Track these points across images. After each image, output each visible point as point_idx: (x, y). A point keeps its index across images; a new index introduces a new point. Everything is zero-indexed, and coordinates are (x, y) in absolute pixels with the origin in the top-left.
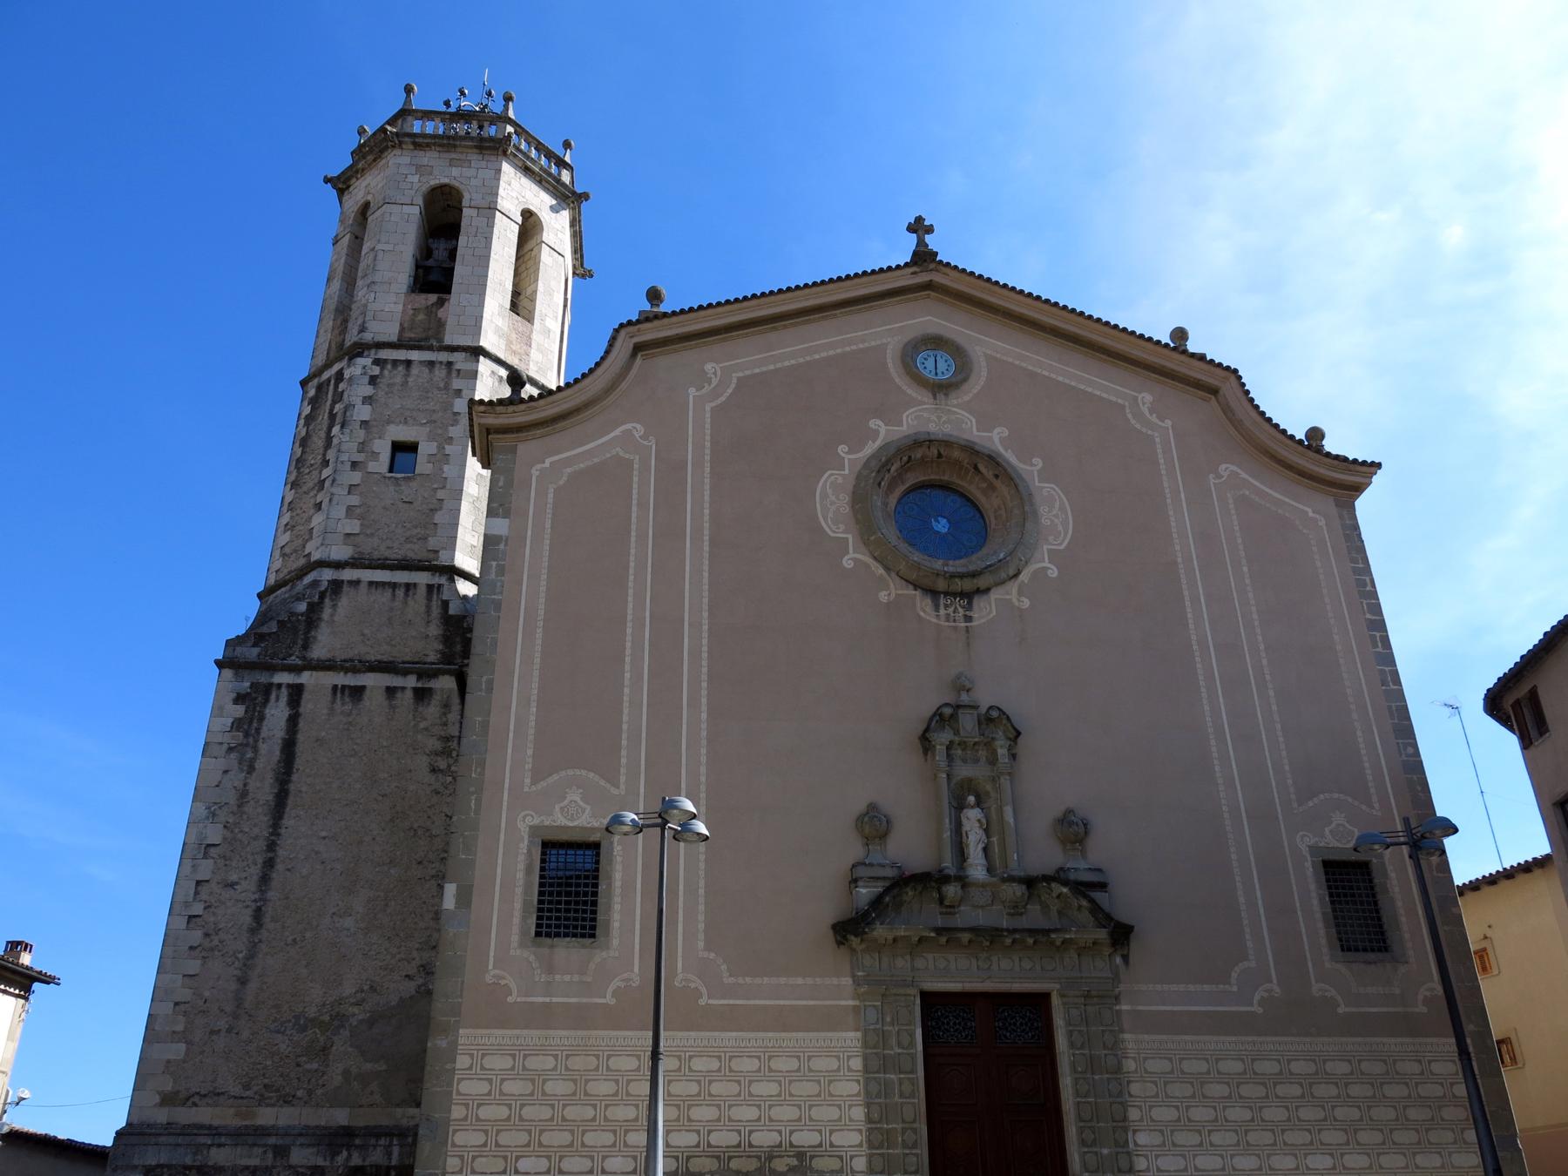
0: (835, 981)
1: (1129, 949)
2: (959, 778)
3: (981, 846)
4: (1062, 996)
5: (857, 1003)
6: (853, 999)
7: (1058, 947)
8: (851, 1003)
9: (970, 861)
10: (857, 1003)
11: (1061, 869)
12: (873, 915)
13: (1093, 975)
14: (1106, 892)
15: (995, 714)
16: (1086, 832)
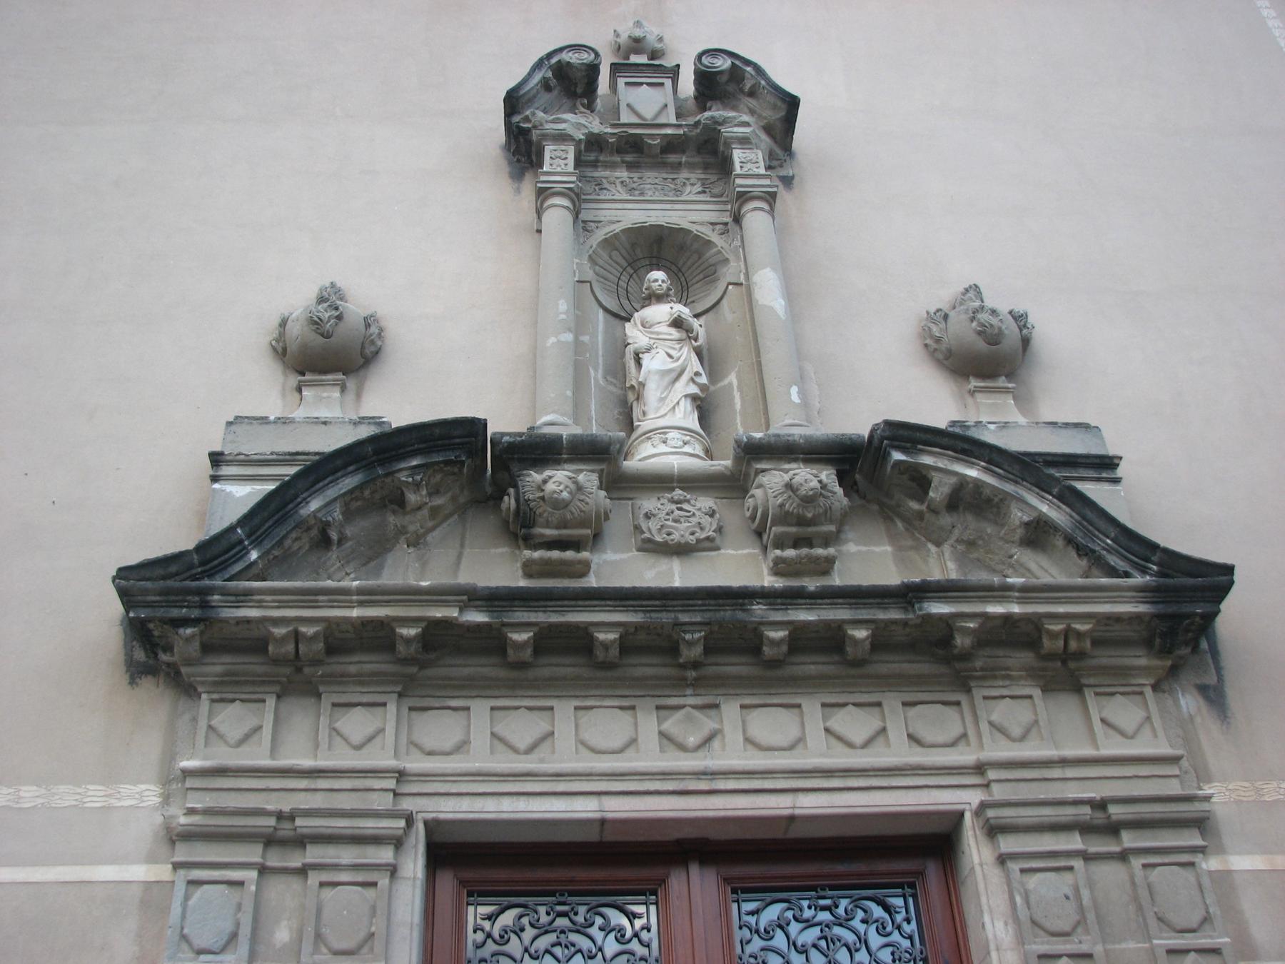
0: (95, 796)
1: (1219, 669)
2: (618, 228)
3: (684, 387)
4: (994, 831)
5: (162, 872)
6: (151, 859)
7: (965, 656)
8: (139, 872)
9: (644, 426)
10: (162, 872)
11: (954, 423)
12: (254, 555)
13: (1106, 752)
14: (1116, 481)
15: (723, 64)
16: (1026, 342)
